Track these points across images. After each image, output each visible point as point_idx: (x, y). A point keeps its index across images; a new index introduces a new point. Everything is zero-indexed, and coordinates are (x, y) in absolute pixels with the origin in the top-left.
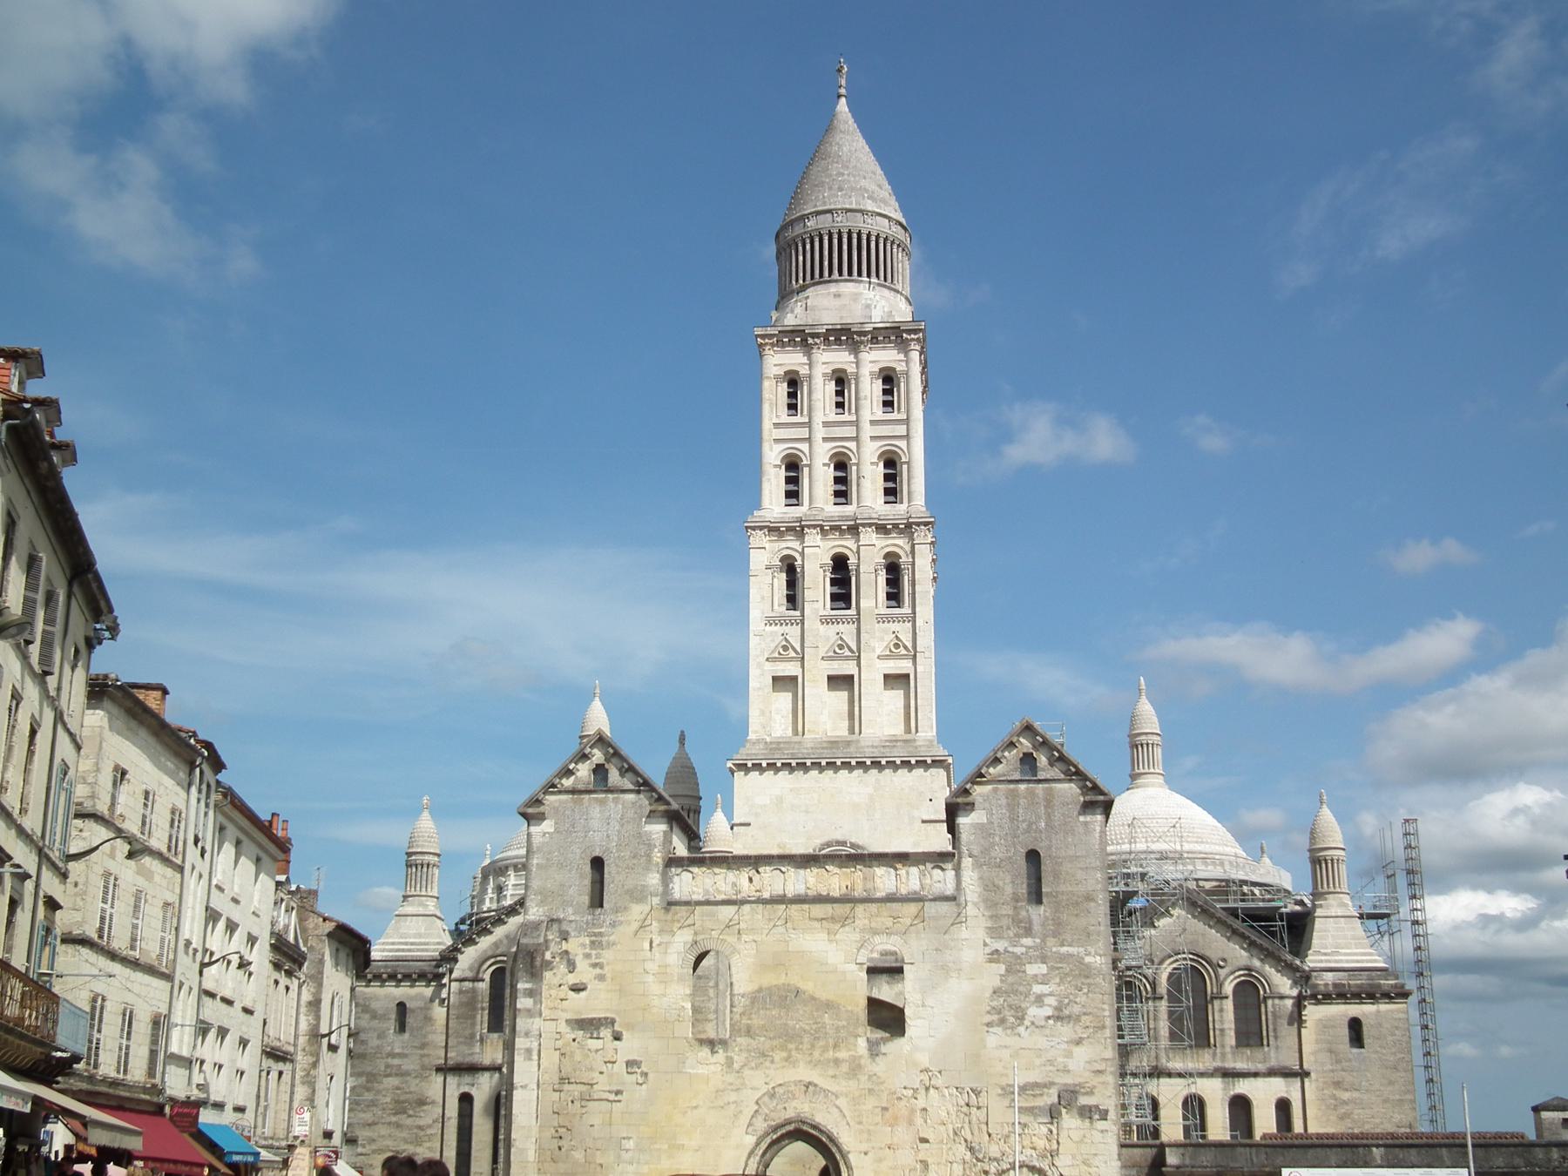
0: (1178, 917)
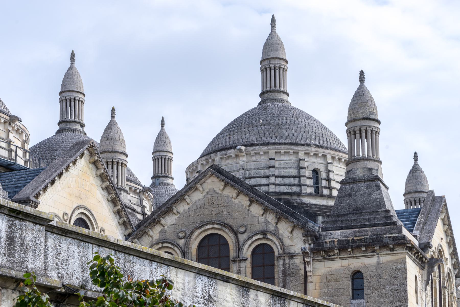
0: (208, 193)
